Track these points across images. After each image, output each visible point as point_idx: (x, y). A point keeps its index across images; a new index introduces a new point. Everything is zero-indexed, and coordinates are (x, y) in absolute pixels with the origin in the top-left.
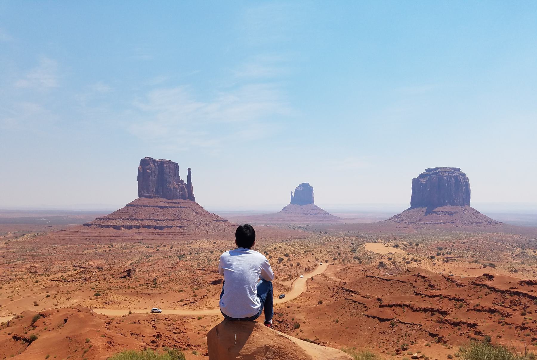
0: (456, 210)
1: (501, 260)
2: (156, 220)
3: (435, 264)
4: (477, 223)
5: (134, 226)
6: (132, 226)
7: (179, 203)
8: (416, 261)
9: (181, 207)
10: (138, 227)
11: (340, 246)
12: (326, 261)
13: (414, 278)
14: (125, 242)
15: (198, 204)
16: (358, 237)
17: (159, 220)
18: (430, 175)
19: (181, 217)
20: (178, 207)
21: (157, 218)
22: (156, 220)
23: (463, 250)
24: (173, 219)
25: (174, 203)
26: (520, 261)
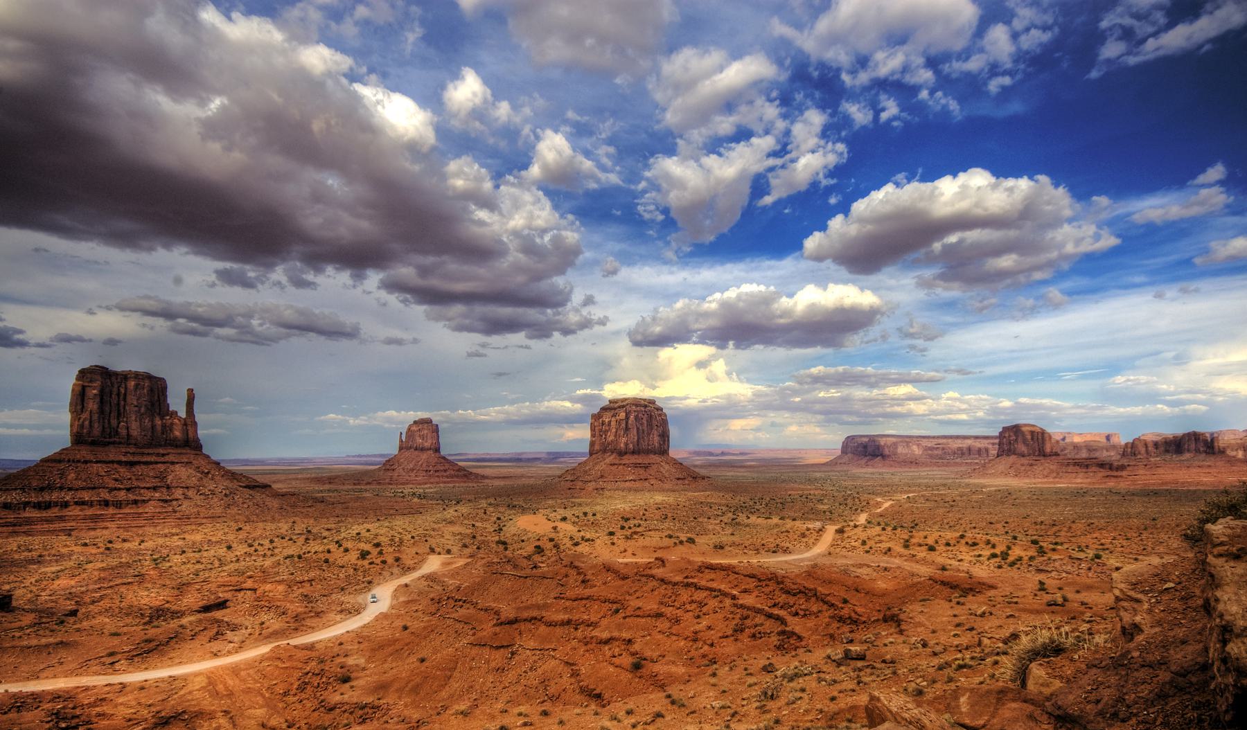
0: (651, 461)
1: (705, 532)
2: (111, 490)
3: (613, 544)
4: (678, 479)
5: (57, 502)
6: (50, 502)
7: (168, 454)
8: (588, 540)
9: (173, 463)
10: (65, 505)
11: (477, 524)
12: (449, 552)
13: (564, 571)
14: (30, 535)
15: (208, 457)
16: (509, 506)
17: (116, 489)
18: (615, 409)
19: (169, 482)
20: (164, 463)
21: (112, 484)
22: (111, 490)
23: (657, 520)
24: (148, 485)
25: (158, 455)
26: (730, 532)
